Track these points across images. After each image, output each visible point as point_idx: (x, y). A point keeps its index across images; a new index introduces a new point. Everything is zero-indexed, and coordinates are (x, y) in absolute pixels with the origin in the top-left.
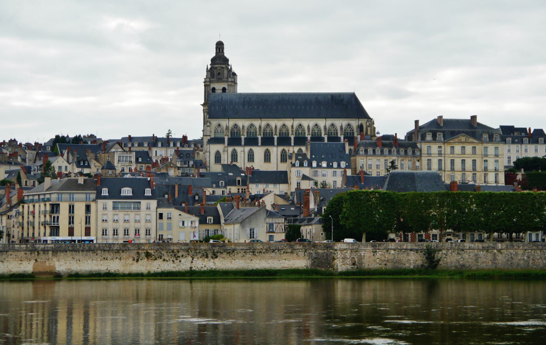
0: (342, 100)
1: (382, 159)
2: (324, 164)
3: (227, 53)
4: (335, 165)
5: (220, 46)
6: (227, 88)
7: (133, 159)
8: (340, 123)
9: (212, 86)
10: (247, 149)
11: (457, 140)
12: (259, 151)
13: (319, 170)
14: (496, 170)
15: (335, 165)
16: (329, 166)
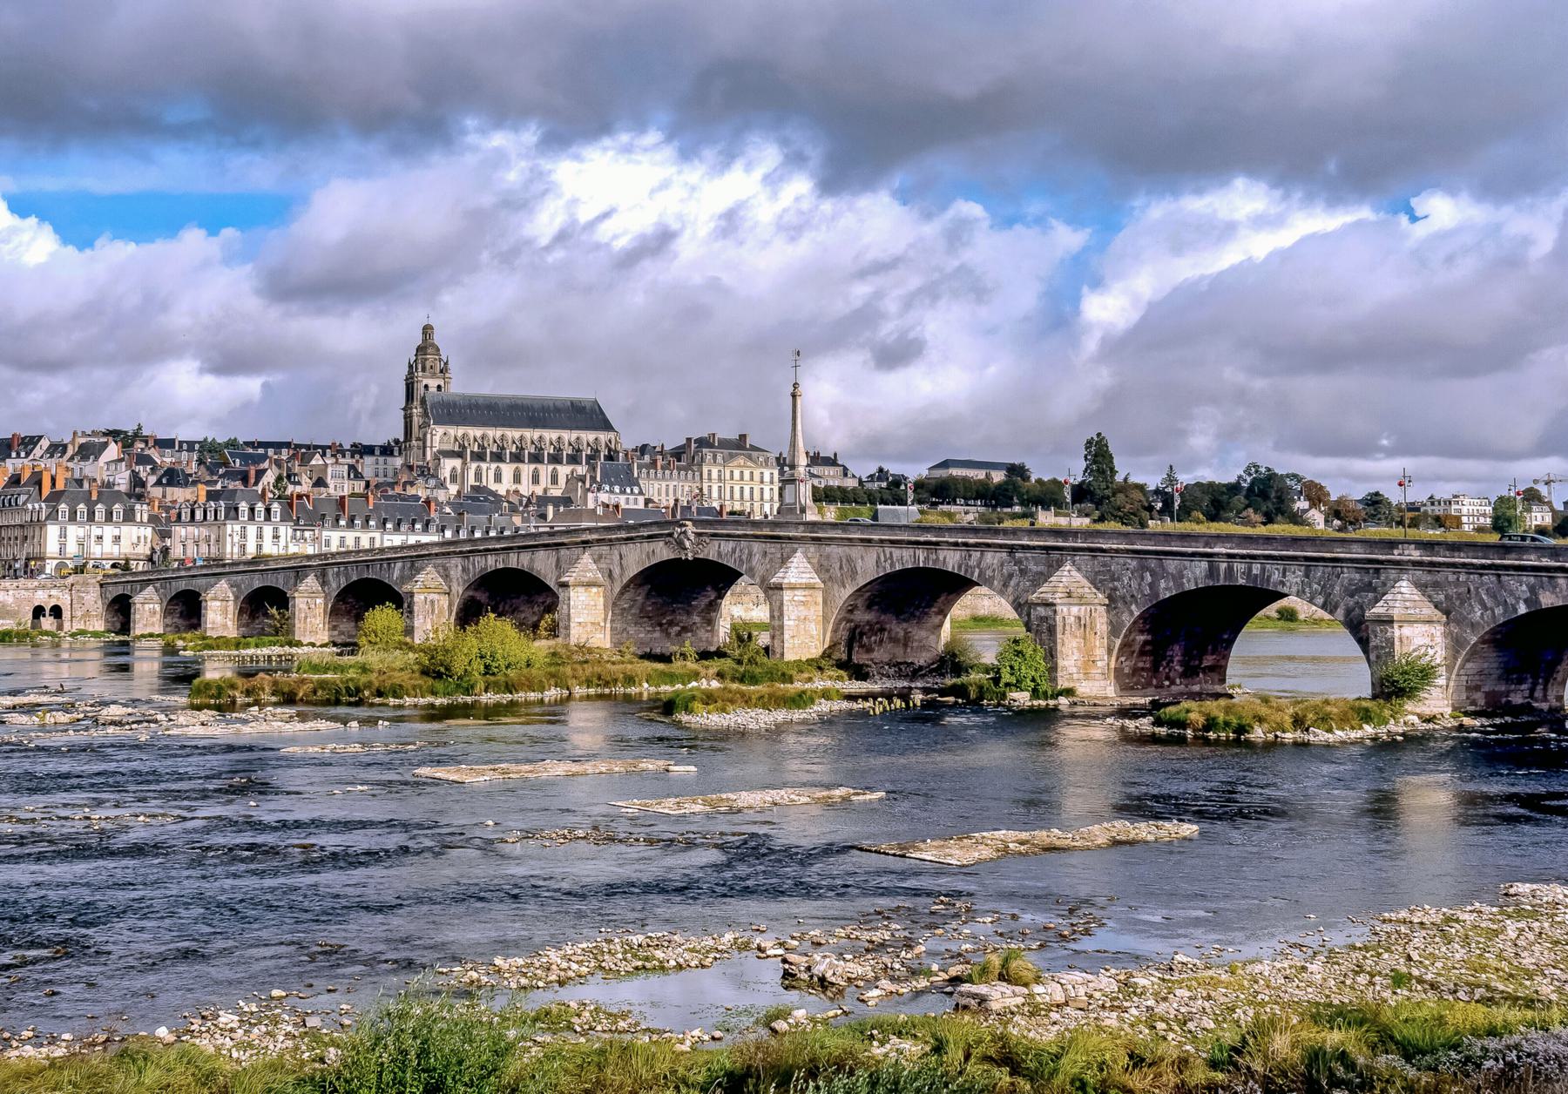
0: (584, 408)
1: (664, 484)
2: (617, 489)
3: (437, 339)
4: (628, 490)
5: (427, 330)
6: (442, 384)
7: (346, 475)
8: (588, 436)
9: (425, 382)
10: (494, 466)
11: (735, 463)
12: (507, 469)
13: (612, 496)
14: (772, 499)
15: (628, 490)
16: (623, 492)
